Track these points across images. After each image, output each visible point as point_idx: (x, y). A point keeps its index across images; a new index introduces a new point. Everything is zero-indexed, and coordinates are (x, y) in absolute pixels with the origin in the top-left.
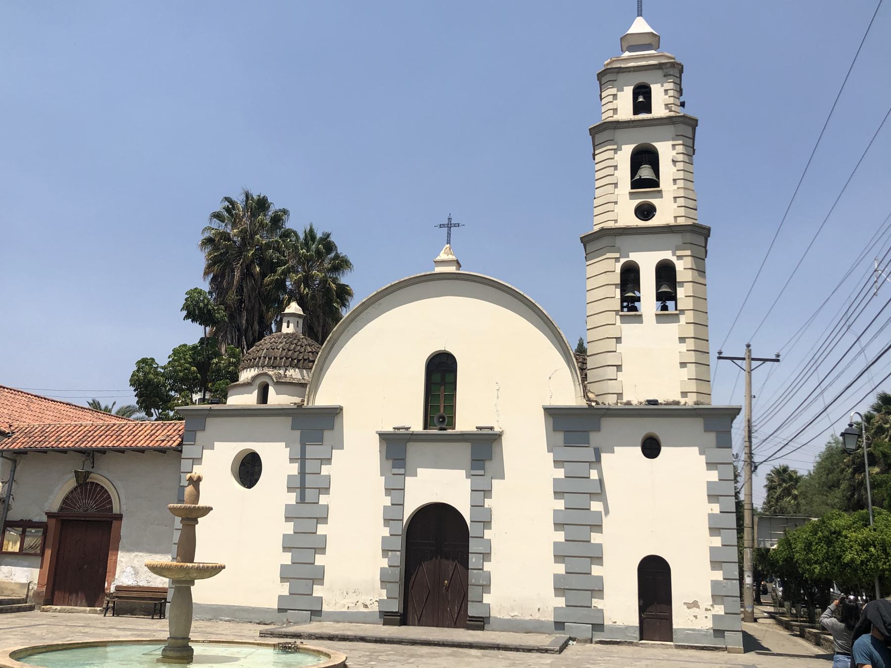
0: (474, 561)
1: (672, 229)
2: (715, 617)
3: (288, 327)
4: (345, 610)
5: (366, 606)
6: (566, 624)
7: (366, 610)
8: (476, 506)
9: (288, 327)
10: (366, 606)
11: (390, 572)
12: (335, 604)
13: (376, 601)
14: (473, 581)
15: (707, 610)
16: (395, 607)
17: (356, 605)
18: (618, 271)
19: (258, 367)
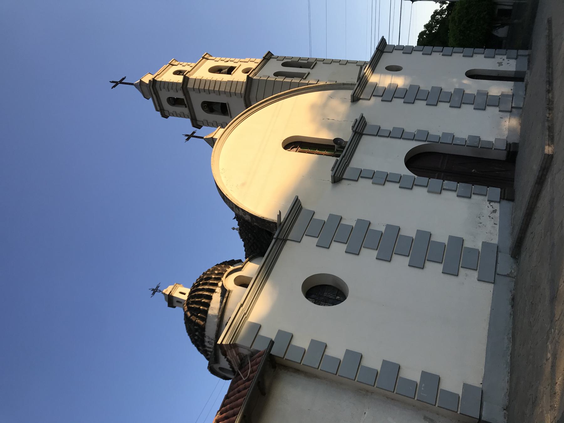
0: (458, 142)
1: (266, 59)
2: (507, 58)
3: (184, 294)
4: (497, 227)
5: (495, 211)
6: (513, 106)
7: (498, 212)
8: (413, 138)
9: (184, 294)
10: (495, 211)
11: (463, 189)
12: (491, 233)
13: (489, 203)
14: (476, 144)
15: (504, 60)
16: (496, 192)
17: (492, 218)
18: (277, 77)
19: (213, 291)
